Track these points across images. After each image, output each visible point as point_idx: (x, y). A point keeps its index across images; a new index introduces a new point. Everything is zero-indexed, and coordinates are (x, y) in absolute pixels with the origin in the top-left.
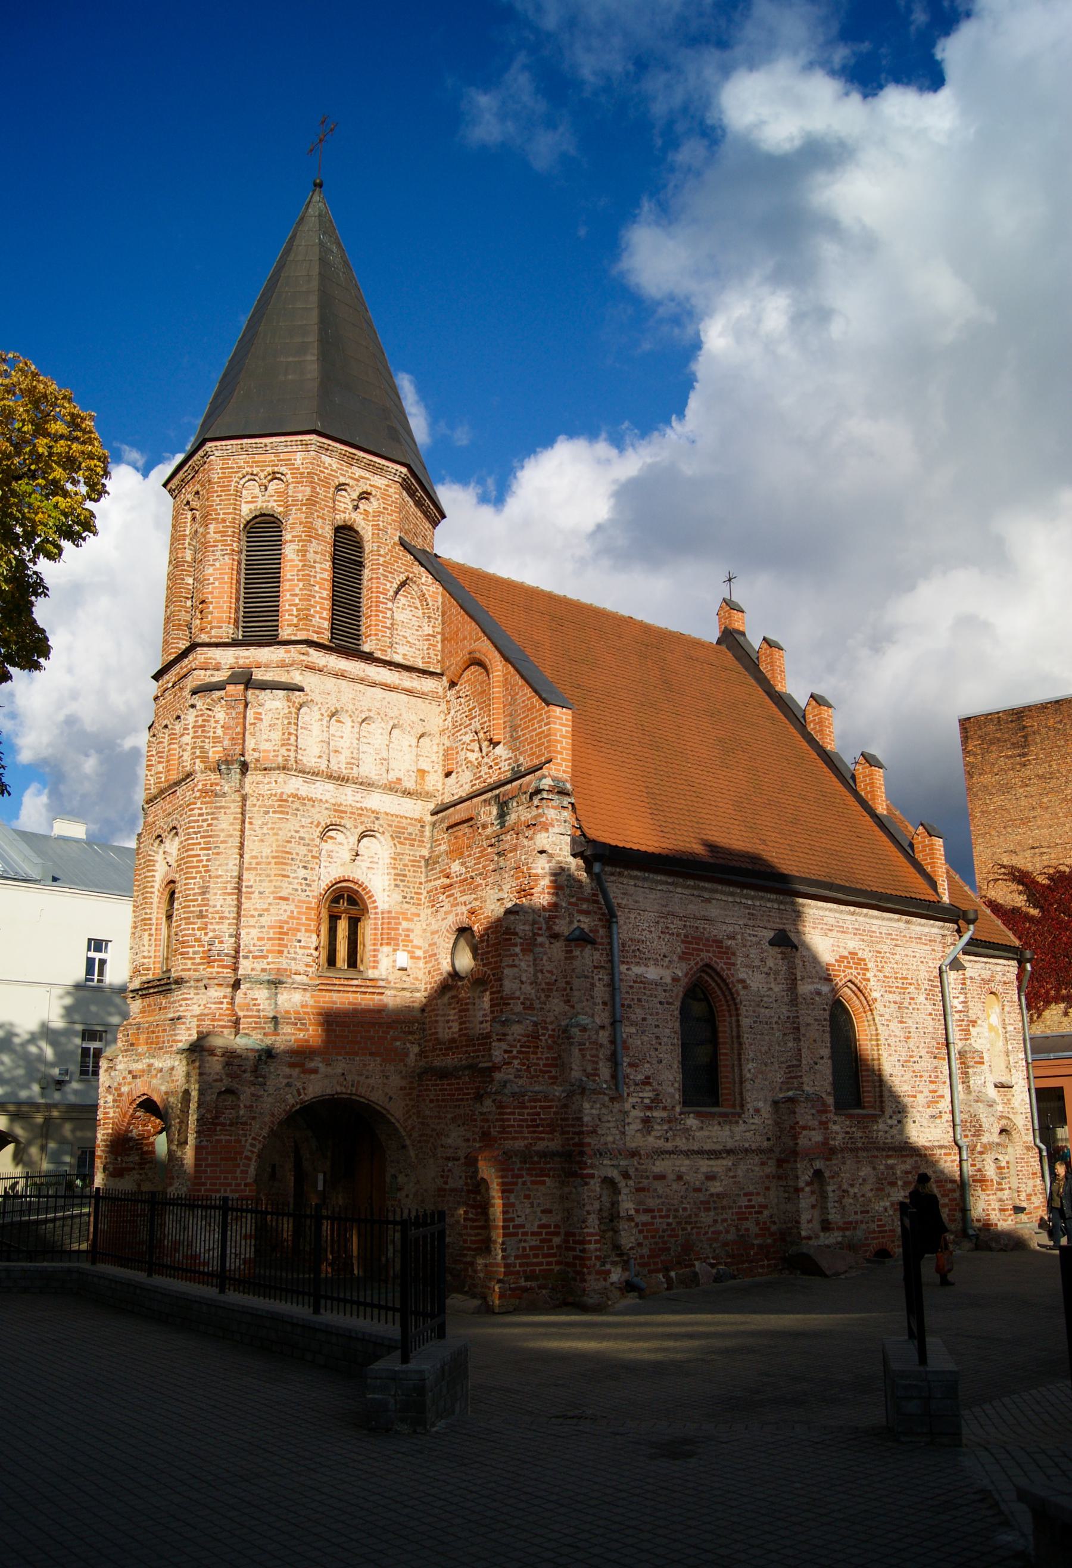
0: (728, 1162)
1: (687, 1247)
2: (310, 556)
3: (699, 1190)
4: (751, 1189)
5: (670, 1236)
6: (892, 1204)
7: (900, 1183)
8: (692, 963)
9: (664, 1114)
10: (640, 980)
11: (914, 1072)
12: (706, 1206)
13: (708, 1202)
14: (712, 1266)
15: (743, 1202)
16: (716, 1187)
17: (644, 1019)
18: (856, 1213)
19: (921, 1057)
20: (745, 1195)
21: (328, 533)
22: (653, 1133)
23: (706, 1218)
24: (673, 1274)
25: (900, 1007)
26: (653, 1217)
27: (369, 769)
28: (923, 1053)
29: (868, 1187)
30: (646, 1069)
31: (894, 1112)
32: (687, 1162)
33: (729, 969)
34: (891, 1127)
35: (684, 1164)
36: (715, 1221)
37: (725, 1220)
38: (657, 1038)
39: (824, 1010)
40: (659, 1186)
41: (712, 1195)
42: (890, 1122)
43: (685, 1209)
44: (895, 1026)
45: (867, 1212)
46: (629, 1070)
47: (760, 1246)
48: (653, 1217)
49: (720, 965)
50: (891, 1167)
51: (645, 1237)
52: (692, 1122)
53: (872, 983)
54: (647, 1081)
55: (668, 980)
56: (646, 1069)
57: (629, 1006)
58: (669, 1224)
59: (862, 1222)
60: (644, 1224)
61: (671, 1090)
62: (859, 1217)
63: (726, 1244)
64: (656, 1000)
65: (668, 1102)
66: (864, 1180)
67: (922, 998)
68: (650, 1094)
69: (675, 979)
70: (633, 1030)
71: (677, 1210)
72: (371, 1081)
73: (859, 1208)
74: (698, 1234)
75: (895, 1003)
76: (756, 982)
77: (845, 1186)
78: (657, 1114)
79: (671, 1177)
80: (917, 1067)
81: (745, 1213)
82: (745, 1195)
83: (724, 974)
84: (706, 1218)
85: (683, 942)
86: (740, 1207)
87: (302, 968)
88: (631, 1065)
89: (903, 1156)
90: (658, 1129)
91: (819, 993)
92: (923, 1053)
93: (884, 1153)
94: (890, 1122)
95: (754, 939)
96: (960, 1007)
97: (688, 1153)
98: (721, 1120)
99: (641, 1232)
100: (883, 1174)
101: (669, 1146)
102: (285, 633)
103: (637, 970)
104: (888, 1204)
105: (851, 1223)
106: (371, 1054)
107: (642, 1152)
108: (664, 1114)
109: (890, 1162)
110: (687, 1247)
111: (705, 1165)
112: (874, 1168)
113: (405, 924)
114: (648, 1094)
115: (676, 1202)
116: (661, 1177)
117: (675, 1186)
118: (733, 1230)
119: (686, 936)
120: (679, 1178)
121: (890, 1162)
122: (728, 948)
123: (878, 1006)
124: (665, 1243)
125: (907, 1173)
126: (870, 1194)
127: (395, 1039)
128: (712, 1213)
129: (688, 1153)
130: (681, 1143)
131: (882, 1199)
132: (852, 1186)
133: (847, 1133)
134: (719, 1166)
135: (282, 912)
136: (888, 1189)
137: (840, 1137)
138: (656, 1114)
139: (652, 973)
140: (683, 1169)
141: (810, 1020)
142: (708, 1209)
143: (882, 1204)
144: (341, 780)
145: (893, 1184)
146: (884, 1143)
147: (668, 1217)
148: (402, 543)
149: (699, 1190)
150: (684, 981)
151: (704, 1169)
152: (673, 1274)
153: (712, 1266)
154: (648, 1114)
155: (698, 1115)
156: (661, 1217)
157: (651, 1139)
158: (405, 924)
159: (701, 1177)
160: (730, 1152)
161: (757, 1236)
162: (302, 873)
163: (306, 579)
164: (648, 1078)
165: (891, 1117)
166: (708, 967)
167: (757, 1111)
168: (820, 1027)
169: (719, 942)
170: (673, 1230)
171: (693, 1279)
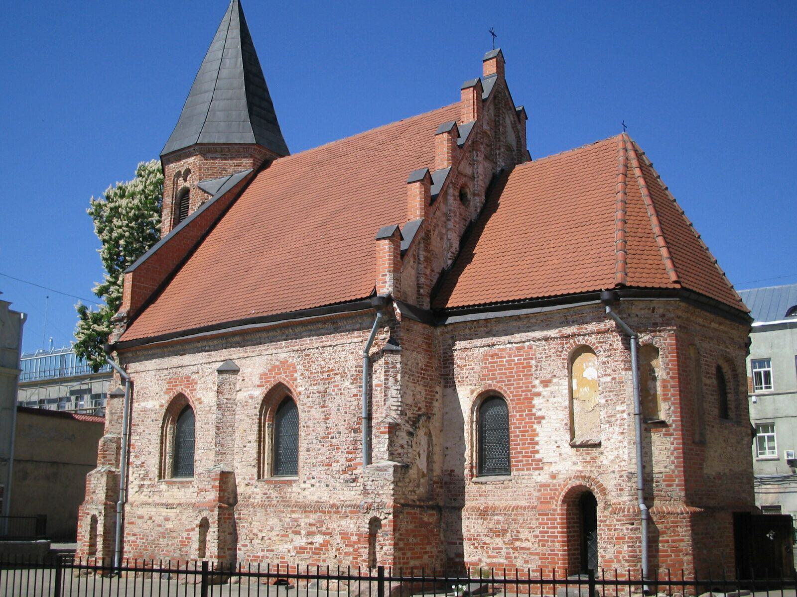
0: (177, 511)
3: (160, 526)
5: (144, 550)
6: (295, 548)
7: (303, 532)
8: (171, 394)
10: (145, 410)
11: (331, 445)
13: (164, 533)
16: (169, 525)
17: (144, 431)
18: (263, 550)
19: (340, 433)
20: (186, 531)
22: (143, 493)
23: (163, 542)
26: (137, 539)
29: (274, 533)
30: (143, 458)
31: (308, 478)
32: (154, 510)
33: (192, 393)
34: (304, 489)
35: (153, 511)
36: (168, 544)
37: (173, 545)
38: (149, 440)
39: (255, 408)
40: (140, 521)
41: (167, 529)
42: (303, 485)
43: (152, 536)
44: (317, 413)
45: (273, 551)
46: (134, 459)
48: (137, 539)
49: (187, 393)
50: (296, 520)
51: (132, 549)
53: (298, 381)
55: (158, 407)
56: (143, 458)
57: (138, 425)
58: (143, 543)
59: (267, 557)
60: (132, 542)
61: (154, 469)
62: (265, 553)
64: (150, 420)
67: (347, 383)
68: (143, 472)
69: (161, 406)
71: (148, 536)
73: (265, 547)
74: (158, 550)
75: (319, 392)
77: (255, 531)
78: (147, 483)
79: (146, 517)
80: (334, 441)
81: (185, 542)
82: (186, 531)
84: (163, 542)
85: (168, 383)
86: (182, 538)
88: (136, 456)
89: (306, 512)
91: (252, 397)
92: (341, 429)
93: (289, 509)
94: (303, 485)
95: (210, 371)
97: (156, 505)
98: (180, 485)
99: (131, 545)
100: (288, 524)
101: (150, 500)
103: (143, 404)
104: (291, 547)
105: (258, 557)
109: (294, 516)
111: (164, 512)
115: (148, 531)
116: (141, 517)
117: (149, 522)
118: (178, 551)
119: (170, 379)
120: (151, 518)
121: (294, 516)
124: (141, 553)
125: (311, 525)
126: (276, 538)
128: (166, 540)
129: (156, 505)
130: (157, 499)
131: (286, 542)
132: (261, 531)
133: (265, 494)
134: (171, 513)
136: (291, 536)
137: (258, 497)
140: (152, 513)
141: (243, 417)
142: (164, 537)
143: (286, 546)
145: (297, 533)
146: (296, 502)
147: (143, 539)
149: (160, 526)
150: (166, 406)
151: (163, 514)
154: (142, 483)
156: (140, 539)
157: (142, 496)
159: (161, 518)
160: (180, 504)
164: (143, 463)
165: (305, 482)
166: (180, 397)
168: (251, 421)
170: (146, 546)
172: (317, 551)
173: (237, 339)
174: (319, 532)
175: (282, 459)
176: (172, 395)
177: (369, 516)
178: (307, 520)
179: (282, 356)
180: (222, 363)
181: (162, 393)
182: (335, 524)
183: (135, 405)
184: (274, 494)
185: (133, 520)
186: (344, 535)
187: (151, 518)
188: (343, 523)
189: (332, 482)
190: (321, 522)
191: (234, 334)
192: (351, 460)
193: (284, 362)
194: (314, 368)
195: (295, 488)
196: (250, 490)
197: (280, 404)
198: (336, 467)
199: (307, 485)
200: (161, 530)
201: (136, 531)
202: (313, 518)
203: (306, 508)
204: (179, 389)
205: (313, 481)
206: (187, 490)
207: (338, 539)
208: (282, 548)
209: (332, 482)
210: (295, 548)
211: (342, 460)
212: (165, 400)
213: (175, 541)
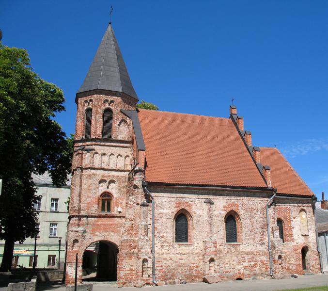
0: (187, 256)
1: (173, 275)
2: (97, 118)
3: (177, 262)
4: (194, 262)
6: (244, 267)
9: (168, 244)
12: (179, 266)
14: (181, 280)
15: (192, 265)
16: (183, 262)
21: (101, 111)
23: (179, 269)
24: (167, 281)
25: (250, 216)
27: (112, 166)
28: (258, 228)
29: (234, 262)
36: (182, 270)
40: (165, 261)
42: (244, 246)
43: (172, 266)
44: (248, 222)
47: (196, 276)
49: (187, 208)
50: (244, 257)
52: (176, 246)
54: (163, 237)
55: (171, 213)
63: (185, 275)
65: (169, 241)
66: (234, 261)
67: (259, 213)
68: (164, 240)
69: (173, 213)
70: (159, 225)
72: (111, 237)
76: (199, 212)
79: (168, 259)
80: (255, 232)
83: (188, 211)
84: (179, 269)
87: (94, 212)
90: (165, 248)
92: (258, 228)
96: (273, 215)
101: (169, 252)
102: (92, 137)
106: (111, 231)
107: (160, 253)
108: (168, 244)
109: (243, 256)
110: (173, 275)
111: (179, 257)
112: (237, 258)
113: (120, 201)
114: (163, 239)
117: (170, 261)
121: (243, 256)
122: (190, 204)
123: (242, 216)
127: (118, 228)
134: (183, 257)
135: (89, 200)
138: (165, 244)
139: (165, 211)
141: (217, 221)
144: (104, 169)
148: (121, 112)
149: (177, 262)
152: (167, 281)
153: (181, 280)
154: (163, 244)
155: (178, 244)
158: (120, 201)
161: (196, 273)
162: (94, 191)
163: (96, 124)
167: (198, 243)
169: (187, 203)
171: (174, 283)
172: (252, 267)
173: (213, 192)
174: (253, 261)
175: (232, 236)
176: (178, 209)
177: (278, 255)
178: (248, 257)
179: (233, 201)
180: (205, 200)
181: (173, 207)
182: (258, 258)
183: (156, 210)
184: (232, 249)
185: (160, 260)
186: (262, 261)
187: (171, 259)
188: (262, 257)
189: (255, 245)
190: (253, 258)
191: (213, 190)
192: (262, 238)
193: (233, 203)
194: (246, 206)
195: (241, 247)
196: (221, 247)
197: (231, 218)
198: (256, 240)
199: (246, 246)
200: (178, 264)
201: (162, 265)
202: (250, 256)
203: (248, 253)
204: (182, 207)
205: (248, 244)
206: (190, 247)
207: (260, 263)
208: (239, 267)
209: (255, 245)
210: (244, 267)
211: (259, 238)
212: (175, 210)
213: (187, 268)
